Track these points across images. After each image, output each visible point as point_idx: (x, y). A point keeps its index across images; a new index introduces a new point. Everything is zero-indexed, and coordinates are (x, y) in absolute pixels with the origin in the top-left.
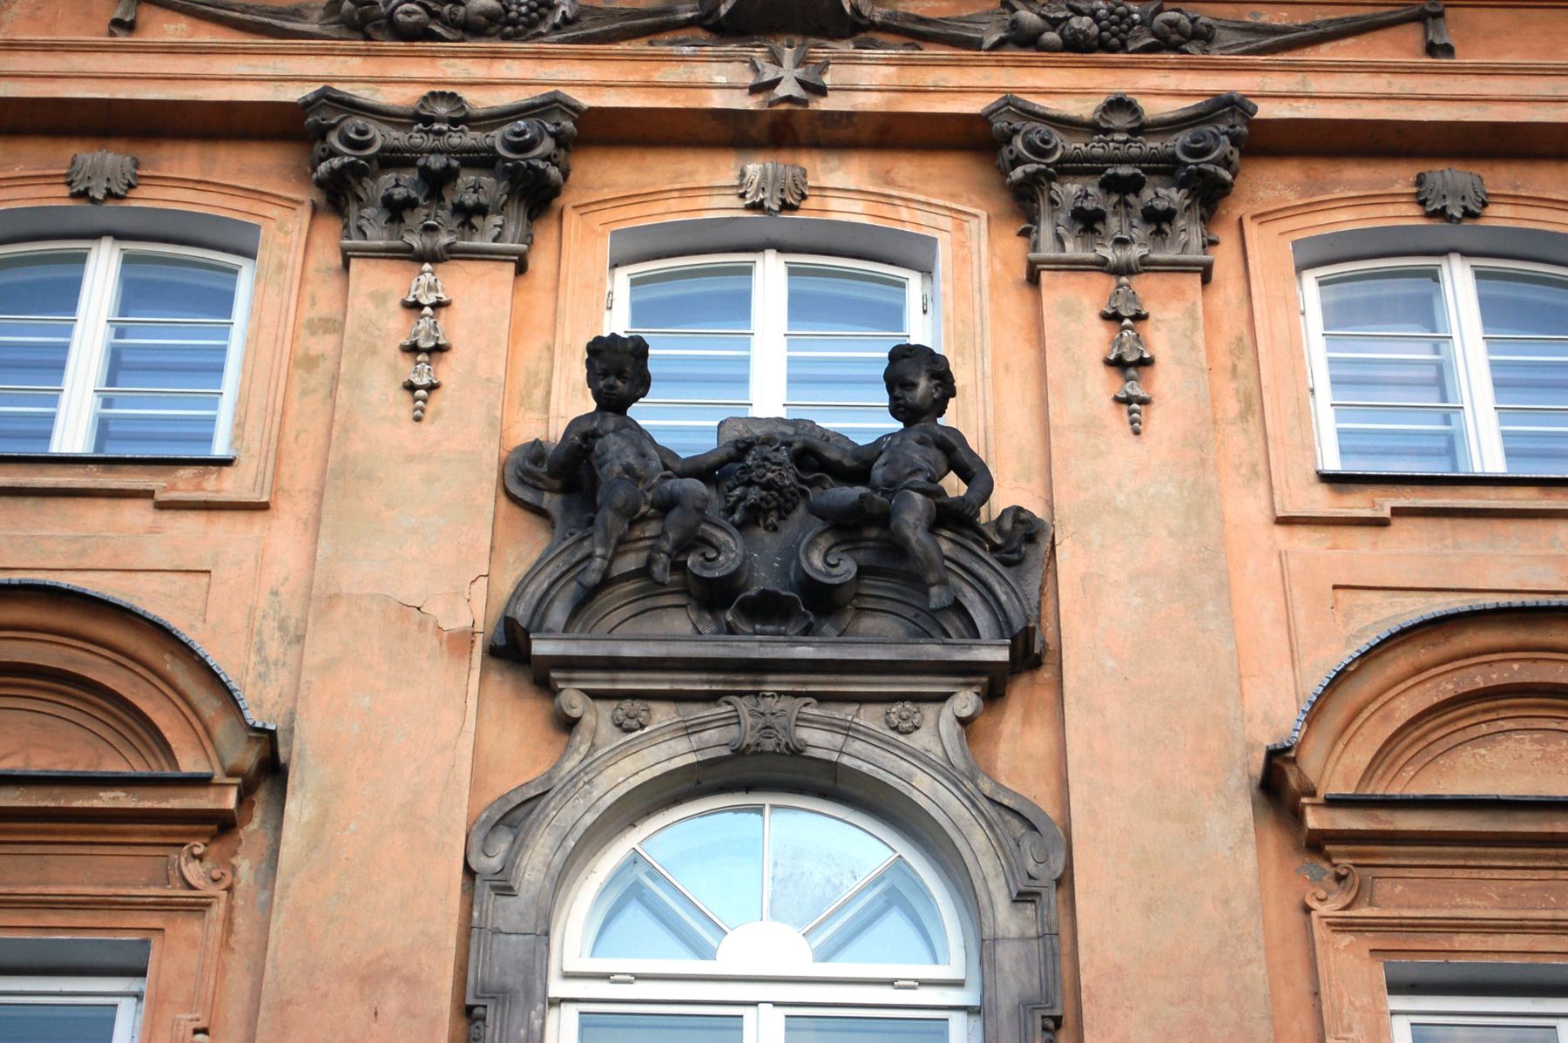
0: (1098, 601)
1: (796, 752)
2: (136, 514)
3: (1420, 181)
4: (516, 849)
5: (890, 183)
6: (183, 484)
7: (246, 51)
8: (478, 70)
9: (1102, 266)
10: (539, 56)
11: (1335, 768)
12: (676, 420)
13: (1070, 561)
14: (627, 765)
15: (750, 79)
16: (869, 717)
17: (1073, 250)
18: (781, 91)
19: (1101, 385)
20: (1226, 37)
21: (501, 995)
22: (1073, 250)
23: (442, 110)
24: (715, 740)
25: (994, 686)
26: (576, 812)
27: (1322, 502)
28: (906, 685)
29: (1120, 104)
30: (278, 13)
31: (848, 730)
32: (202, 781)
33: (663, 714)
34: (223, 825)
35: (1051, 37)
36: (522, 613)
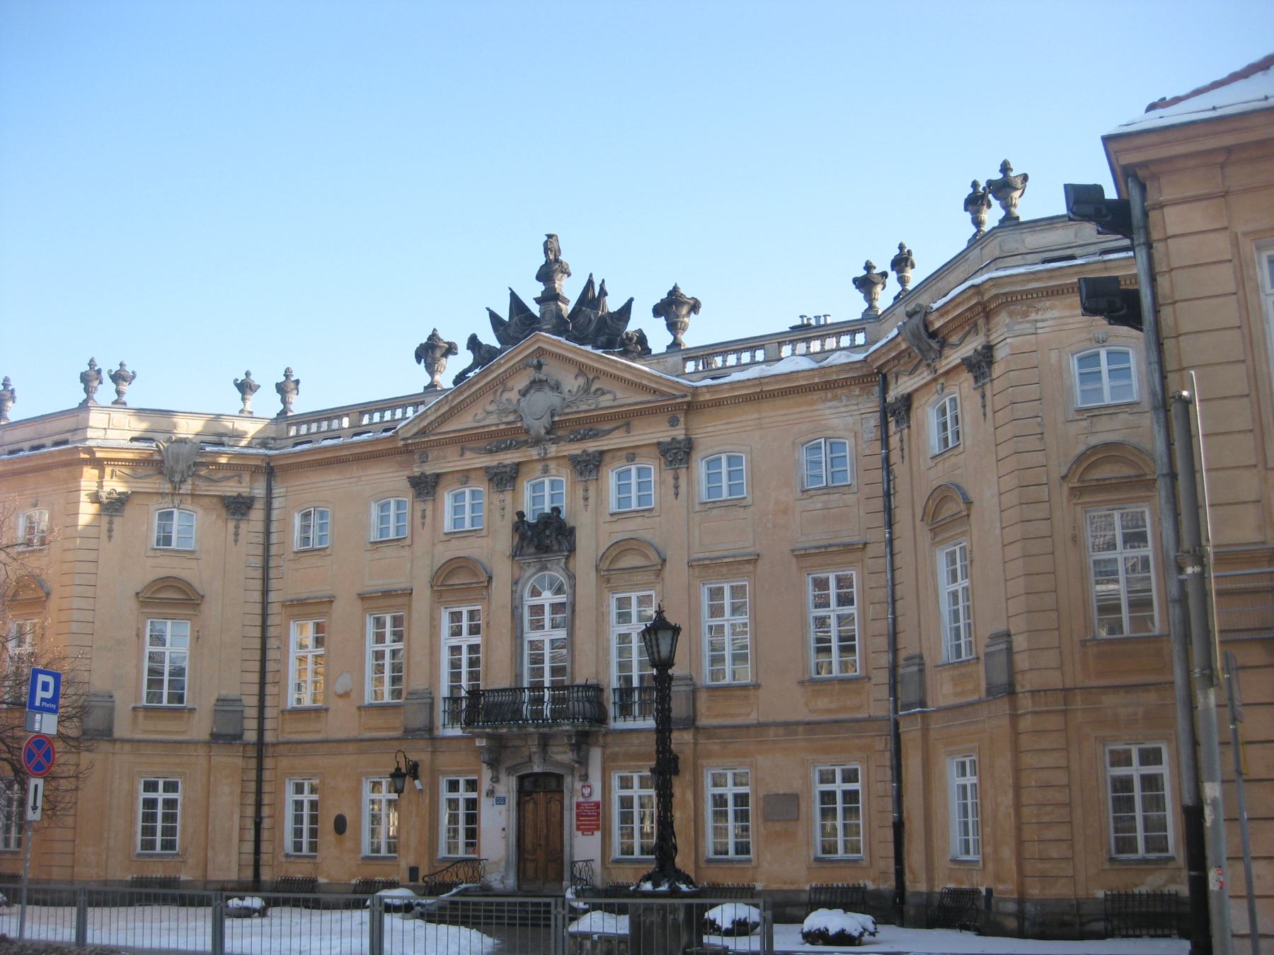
11: (604, 565)
25: (567, 558)
26: (522, 581)
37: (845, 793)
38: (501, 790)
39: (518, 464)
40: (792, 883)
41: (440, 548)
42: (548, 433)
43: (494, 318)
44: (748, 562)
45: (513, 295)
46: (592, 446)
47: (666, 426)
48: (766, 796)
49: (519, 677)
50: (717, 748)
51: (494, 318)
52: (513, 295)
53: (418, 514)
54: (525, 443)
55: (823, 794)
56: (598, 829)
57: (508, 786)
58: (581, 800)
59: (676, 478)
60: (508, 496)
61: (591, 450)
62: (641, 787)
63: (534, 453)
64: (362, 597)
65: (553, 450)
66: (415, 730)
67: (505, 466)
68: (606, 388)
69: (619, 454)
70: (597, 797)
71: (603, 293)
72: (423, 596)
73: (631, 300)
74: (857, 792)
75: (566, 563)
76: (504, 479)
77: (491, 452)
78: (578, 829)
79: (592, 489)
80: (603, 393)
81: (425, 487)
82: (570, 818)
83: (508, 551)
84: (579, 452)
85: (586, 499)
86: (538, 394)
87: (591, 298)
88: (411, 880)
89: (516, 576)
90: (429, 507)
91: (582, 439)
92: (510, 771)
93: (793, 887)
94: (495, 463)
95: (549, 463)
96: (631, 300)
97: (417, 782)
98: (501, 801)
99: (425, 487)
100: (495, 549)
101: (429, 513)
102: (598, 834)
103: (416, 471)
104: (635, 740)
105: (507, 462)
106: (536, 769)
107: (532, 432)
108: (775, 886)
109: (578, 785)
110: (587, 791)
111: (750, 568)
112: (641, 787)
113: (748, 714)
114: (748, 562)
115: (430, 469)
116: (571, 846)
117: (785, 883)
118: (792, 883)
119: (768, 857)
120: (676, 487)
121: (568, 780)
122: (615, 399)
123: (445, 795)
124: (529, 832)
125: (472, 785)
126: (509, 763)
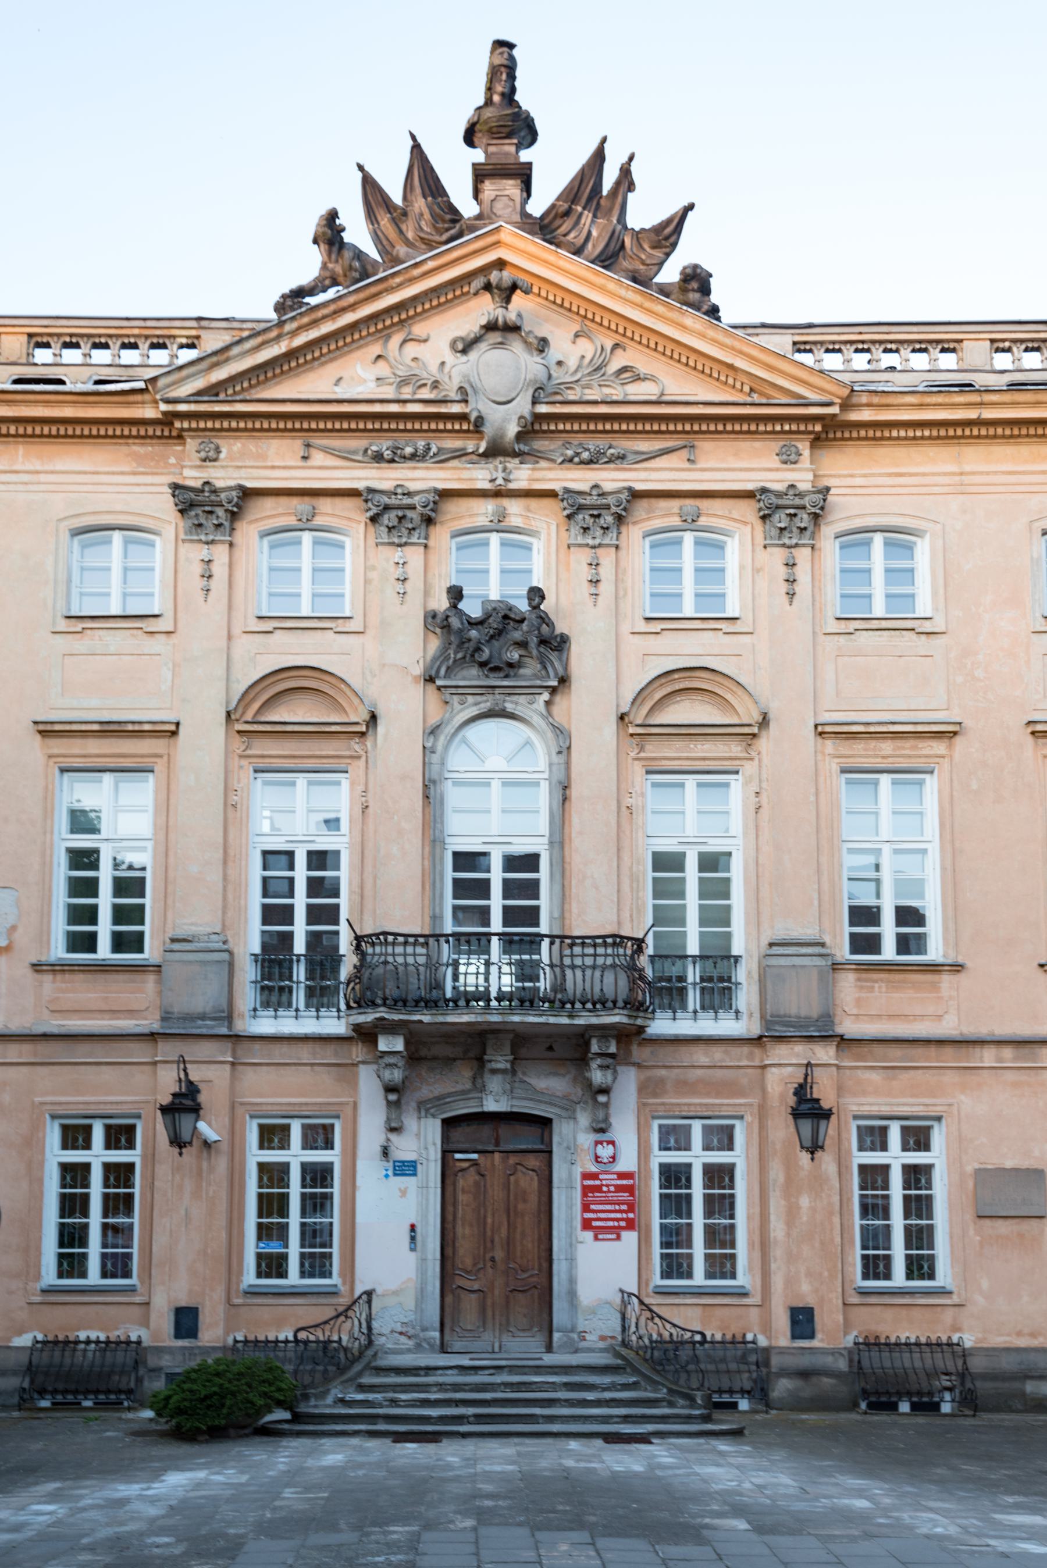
0: (583, 658)
1: (504, 710)
2: (330, 633)
3: (681, 508)
4: (436, 740)
5: (529, 510)
6: (341, 626)
7: (342, 468)
8: (410, 474)
9: (587, 545)
10: (427, 468)
12: (472, 608)
13: (575, 649)
14: (461, 715)
15: (489, 477)
16: (522, 699)
17: (580, 540)
18: (498, 482)
19: (586, 589)
20: (631, 457)
21: (434, 782)
22: (580, 540)
23: (399, 491)
24: (485, 707)
25: (553, 691)
26: (449, 729)
27: (643, 627)
28: (532, 690)
29: (596, 486)
30: (349, 452)
31: (516, 703)
32: (357, 723)
33: (470, 699)
34: (363, 734)
35: (576, 460)
36: (433, 673)
37: (109, 1168)
38: (405, 1148)
39: (445, 494)
40: (1033, 1335)
41: (244, 645)
42: (520, 437)
43: (370, 187)
44: (939, 735)
45: (417, 148)
46: (612, 479)
47: (775, 462)
48: (978, 1172)
49: (436, 919)
50: (875, 1077)
51: (372, 191)
52: (417, 148)
53: (198, 569)
54: (460, 454)
55: (66, 1168)
56: (630, 1225)
57: (422, 1139)
58: (593, 1168)
59: (791, 565)
60: (414, 556)
61: (608, 487)
62: (108, 1146)
63: (480, 476)
64: (47, 731)
65: (523, 475)
66: (189, 1018)
67: (409, 494)
68: (643, 369)
69: (663, 504)
70: (628, 1162)
71: (626, 180)
72: (205, 743)
73: (691, 207)
74: (130, 1167)
75: (548, 703)
76: (404, 520)
77: (378, 457)
78: (587, 1225)
79: (607, 558)
80: (638, 378)
81: (210, 512)
82: (566, 1205)
83: (418, 670)
84: (584, 487)
85: (595, 582)
86: (498, 353)
87: (595, 190)
88: (178, 1334)
89: (433, 721)
90: (220, 553)
91: (591, 462)
92: (425, 1108)
93: (1035, 1343)
94: (387, 485)
95: (506, 502)
96: (691, 207)
97: (202, 1125)
98: (406, 1169)
99: (210, 512)
100: (386, 660)
101: (219, 570)
102: (630, 1238)
103: (192, 477)
104: (701, 1056)
105: (413, 486)
106: (491, 1105)
107: (488, 430)
108: (998, 1341)
109: (586, 1139)
110: (605, 1152)
111: (939, 747)
112: (108, 1146)
113: (940, 1017)
114: (939, 735)
115: (225, 476)
116: (572, 1260)
117: (1019, 1334)
118: (1033, 1335)
119: (985, 1284)
120: (791, 581)
121: (562, 1131)
122: (662, 394)
123: (255, 1155)
124: (464, 1232)
125: (319, 1136)
126: (426, 1091)
